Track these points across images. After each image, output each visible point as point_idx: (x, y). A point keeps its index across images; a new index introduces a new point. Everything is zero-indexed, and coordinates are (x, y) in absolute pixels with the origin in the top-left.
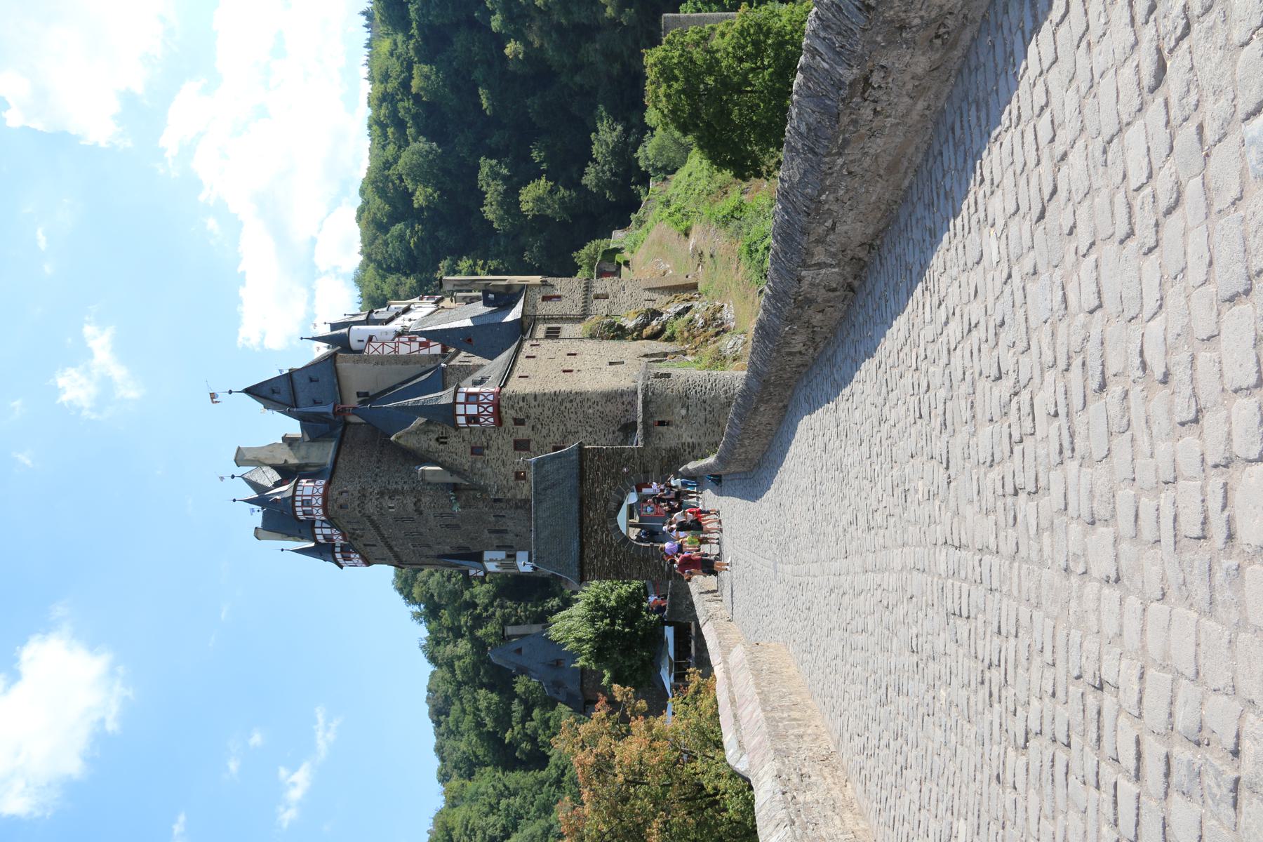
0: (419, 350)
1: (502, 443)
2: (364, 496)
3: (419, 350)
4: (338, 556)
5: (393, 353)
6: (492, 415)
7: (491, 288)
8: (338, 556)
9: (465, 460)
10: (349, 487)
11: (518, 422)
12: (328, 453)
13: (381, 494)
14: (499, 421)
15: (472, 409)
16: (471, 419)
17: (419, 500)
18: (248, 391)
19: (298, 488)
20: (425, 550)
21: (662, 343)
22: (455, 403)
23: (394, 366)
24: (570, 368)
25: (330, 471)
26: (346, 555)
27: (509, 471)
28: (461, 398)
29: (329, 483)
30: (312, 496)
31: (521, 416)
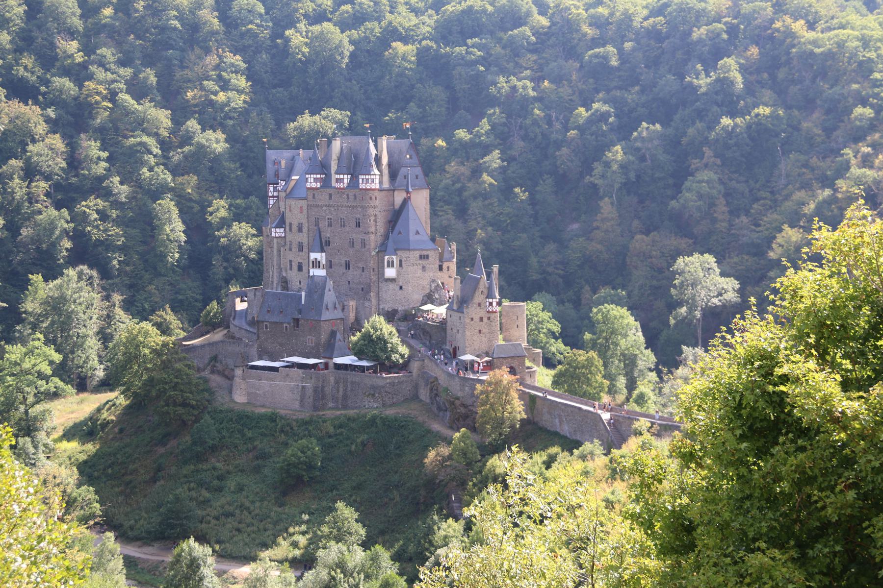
1: (482, 313)
8: (318, 176)
11: (489, 318)
13: (375, 216)
14: (488, 312)
15: (494, 304)
16: (491, 304)
27: (474, 316)
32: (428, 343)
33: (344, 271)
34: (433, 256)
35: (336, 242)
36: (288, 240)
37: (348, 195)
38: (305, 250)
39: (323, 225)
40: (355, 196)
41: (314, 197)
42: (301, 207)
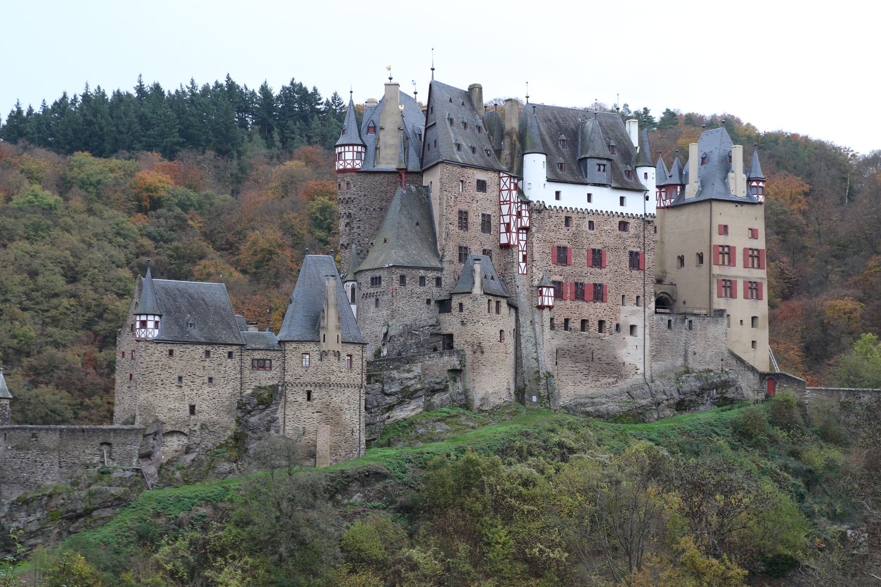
0: (504, 223)
2: (347, 202)
3: (504, 223)
5: (502, 200)
10: (354, 189)
12: (390, 163)
15: (138, 325)
17: (346, 248)
18: (430, 85)
19: (351, 148)
21: (226, 438)
22: (140, 315)
24: (184, 381)
25: (371, 169)
28: (143, 318)
30: (345, 160)
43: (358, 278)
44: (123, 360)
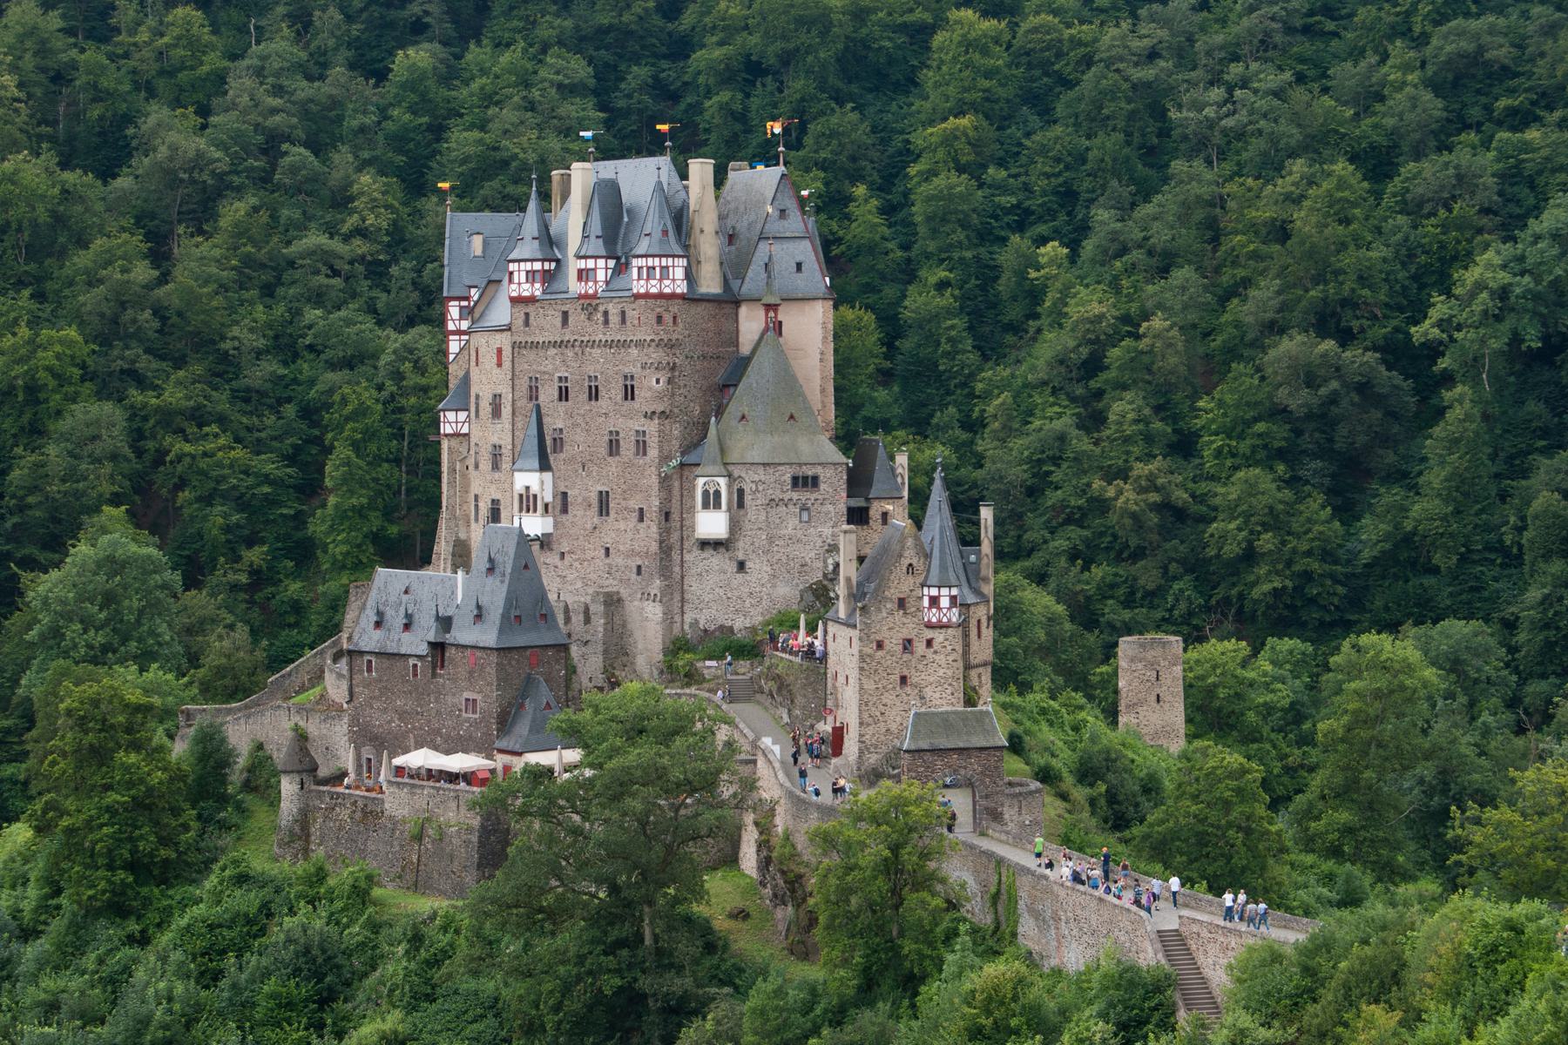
1: (909, 628)
4: (537, 266)
6: (940, 621)
7: (985, 561)
8: (537, 266)
9: (893, 593)
11: (929, 643)
13: (673, 369)
14: (930, 626)
15: (945, 602)
16: (934, 601)
20: (548, 394)
23: (818, 375)
26: (538, 276)
27: (884, 634)
28: (954, 591)
29: (682, 297)
31: (936, 645)
32: (786, 719)
33: (596, 520)
34: (834, 484)
35: (577, 442)
36: (473, 440)
37: (606, 313)
38: (506, 464)
39: (548, 394)
40: (623, 313)
41: (527, 323)
42: (499, 351)
43: (731, 468)
44: (880, 653)
